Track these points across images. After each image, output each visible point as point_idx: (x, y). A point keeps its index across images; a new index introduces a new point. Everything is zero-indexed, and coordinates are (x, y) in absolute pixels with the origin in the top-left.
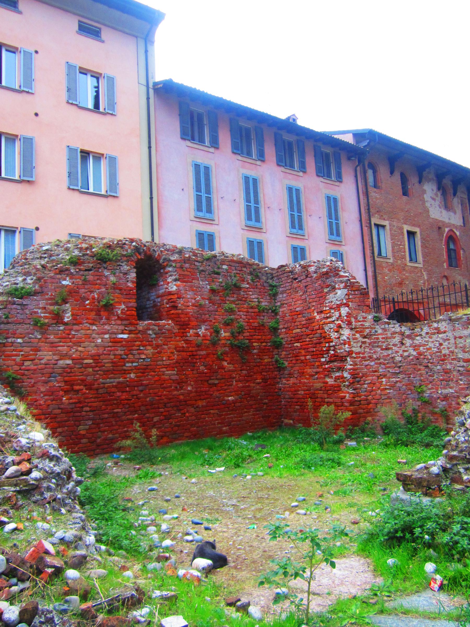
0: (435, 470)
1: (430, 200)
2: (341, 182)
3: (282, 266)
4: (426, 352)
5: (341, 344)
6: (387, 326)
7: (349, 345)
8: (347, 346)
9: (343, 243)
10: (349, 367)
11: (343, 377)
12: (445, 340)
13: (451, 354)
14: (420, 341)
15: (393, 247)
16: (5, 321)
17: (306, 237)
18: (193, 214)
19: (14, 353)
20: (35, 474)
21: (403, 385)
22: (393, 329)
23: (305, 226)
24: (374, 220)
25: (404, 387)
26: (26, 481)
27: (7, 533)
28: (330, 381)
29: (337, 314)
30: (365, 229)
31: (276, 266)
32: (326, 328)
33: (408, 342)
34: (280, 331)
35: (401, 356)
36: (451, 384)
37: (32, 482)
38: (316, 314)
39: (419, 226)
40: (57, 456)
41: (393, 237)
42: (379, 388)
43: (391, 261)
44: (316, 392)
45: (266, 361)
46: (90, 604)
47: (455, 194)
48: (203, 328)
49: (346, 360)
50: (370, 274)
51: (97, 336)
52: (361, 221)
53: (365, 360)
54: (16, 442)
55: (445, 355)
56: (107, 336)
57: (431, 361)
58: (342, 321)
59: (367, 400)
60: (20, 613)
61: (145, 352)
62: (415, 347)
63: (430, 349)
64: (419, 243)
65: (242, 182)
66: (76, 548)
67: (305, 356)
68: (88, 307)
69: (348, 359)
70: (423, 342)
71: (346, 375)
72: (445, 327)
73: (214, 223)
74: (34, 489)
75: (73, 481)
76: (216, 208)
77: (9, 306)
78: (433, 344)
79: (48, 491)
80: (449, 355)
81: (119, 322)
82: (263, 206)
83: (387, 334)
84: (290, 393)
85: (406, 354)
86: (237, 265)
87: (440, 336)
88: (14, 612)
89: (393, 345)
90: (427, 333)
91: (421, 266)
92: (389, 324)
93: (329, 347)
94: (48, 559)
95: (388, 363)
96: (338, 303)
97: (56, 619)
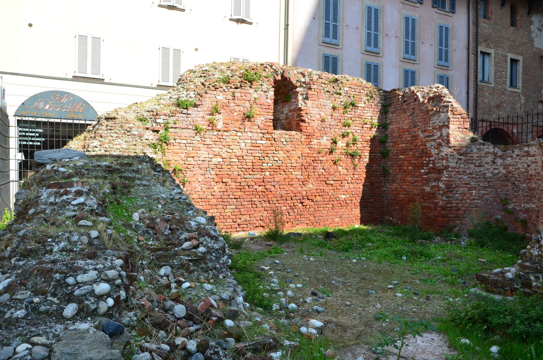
0: (509, 275)
1: (536, 30)
2: (454, 13)
3: (395, 90)
4: (515, 171)
5: (440, 159)
6: (482, 146)
7: (447, 160)
8: (444, 161)
9: (450, 68)
10: (444, 179)
11: (438, 186)
12: (533, 162)
13: (537, 175)
14: (510, 162)
15: (495, 73)
16: (174, 126)
17: (417, 62)
18: (321, 39)
19: (180, 151)
20: (202, 249)
21: (491, 197)
22: (487, 150)
23: (417, 52)
24: (481, 48)
25: (491, 199)
26: (196, 253)
27: (184, 289)
28: (427, 189)
29: (439, 134)
30: (472, 56)
31: (389, 89)
32: (428, 145)
33: (499, 161)
34: (388, 144)
35: (492, 173)
36: (534, 200)
37: (200, 255)
38: (420, 133)
39: (522, 55)
40: (216, 236)
41: (496, 64)
42: (469, 198)
43: (492, 85)
44: (414, 197)
45: (374, 168)
46: (242, 345)
48: (325, 138)
49: (443, 172)
50: (472, 96)
51: (241, 141)
52: (468, 49)
53: (459, 174)
54: (188, 224)
55: (531, 175)
56: (249, 141)
57: (518, 179)
58: (442, 140)
59: (457, 207)
60: (197, 345)
61: (278, 155)
62: (505, 167)
63: (519, 169)
64: (521, 71)
65: (366, 12)
66: (230, 305)
67: (408, 167)
68: (236, 117)
69: (445, 172)
70: (513, 163)
71: (441, 185)
72: (535, 151)
73: (338, 47)
74: (201, 259)
75: (226, 254)
76: (341, 34)
77: (178, 115)
78: (521, 165)
79: (210, 262)
80: (535, 175)
81: (259, 131)
82: (382, 34)
83: (481, 154)
84: (392, 196)
85: (496, 171)
86: (357, 87)
87: (529, 158)
88: (193, 345)
89: (485, 163)
90: (518, 155)
91: (520, 91)
92: (484, 145)
93: (429, 160)
94: (213, 311)
95: (479, 178)
96: (441, 124)
97: (221, 353)
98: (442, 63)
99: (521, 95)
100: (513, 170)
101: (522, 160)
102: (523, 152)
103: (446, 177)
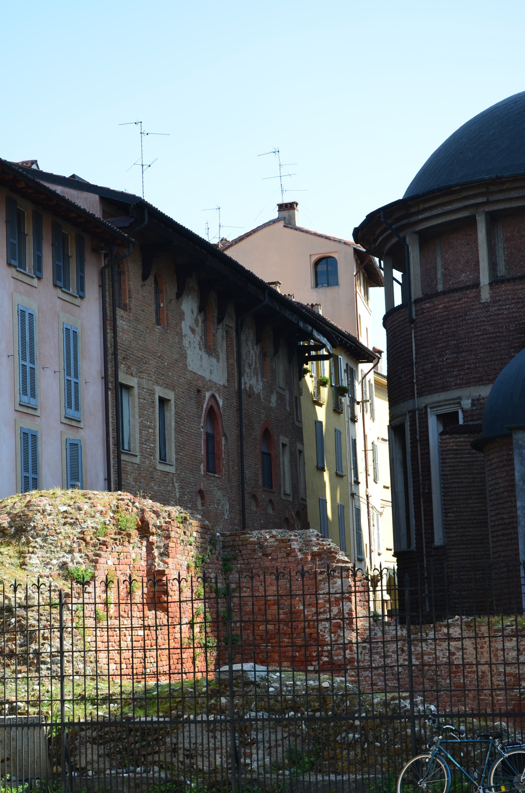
2: (82, 298)
9: (81, 425)
39: (172, 388)
47: (220, 320)
64: (173, 423)
91: (172, 470)
98: (25, 399)
99: (175, 480)
100: (430, 660)
101: (442, 647)
102: (441, 635)
103: (352, 676)
